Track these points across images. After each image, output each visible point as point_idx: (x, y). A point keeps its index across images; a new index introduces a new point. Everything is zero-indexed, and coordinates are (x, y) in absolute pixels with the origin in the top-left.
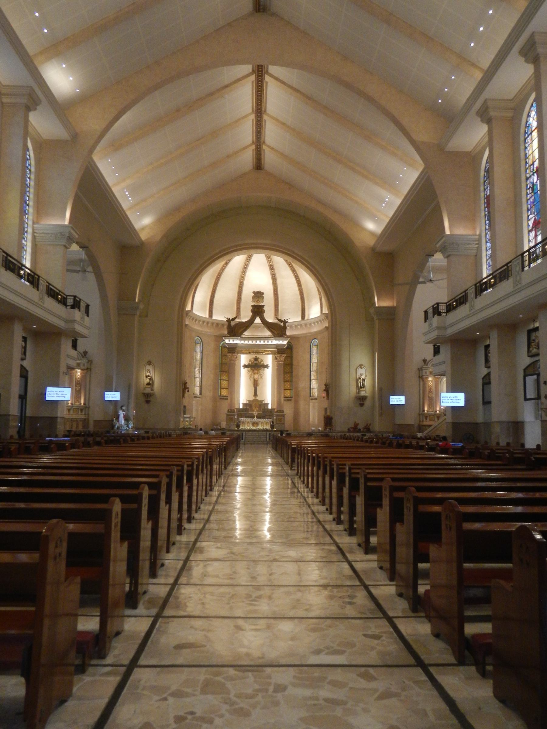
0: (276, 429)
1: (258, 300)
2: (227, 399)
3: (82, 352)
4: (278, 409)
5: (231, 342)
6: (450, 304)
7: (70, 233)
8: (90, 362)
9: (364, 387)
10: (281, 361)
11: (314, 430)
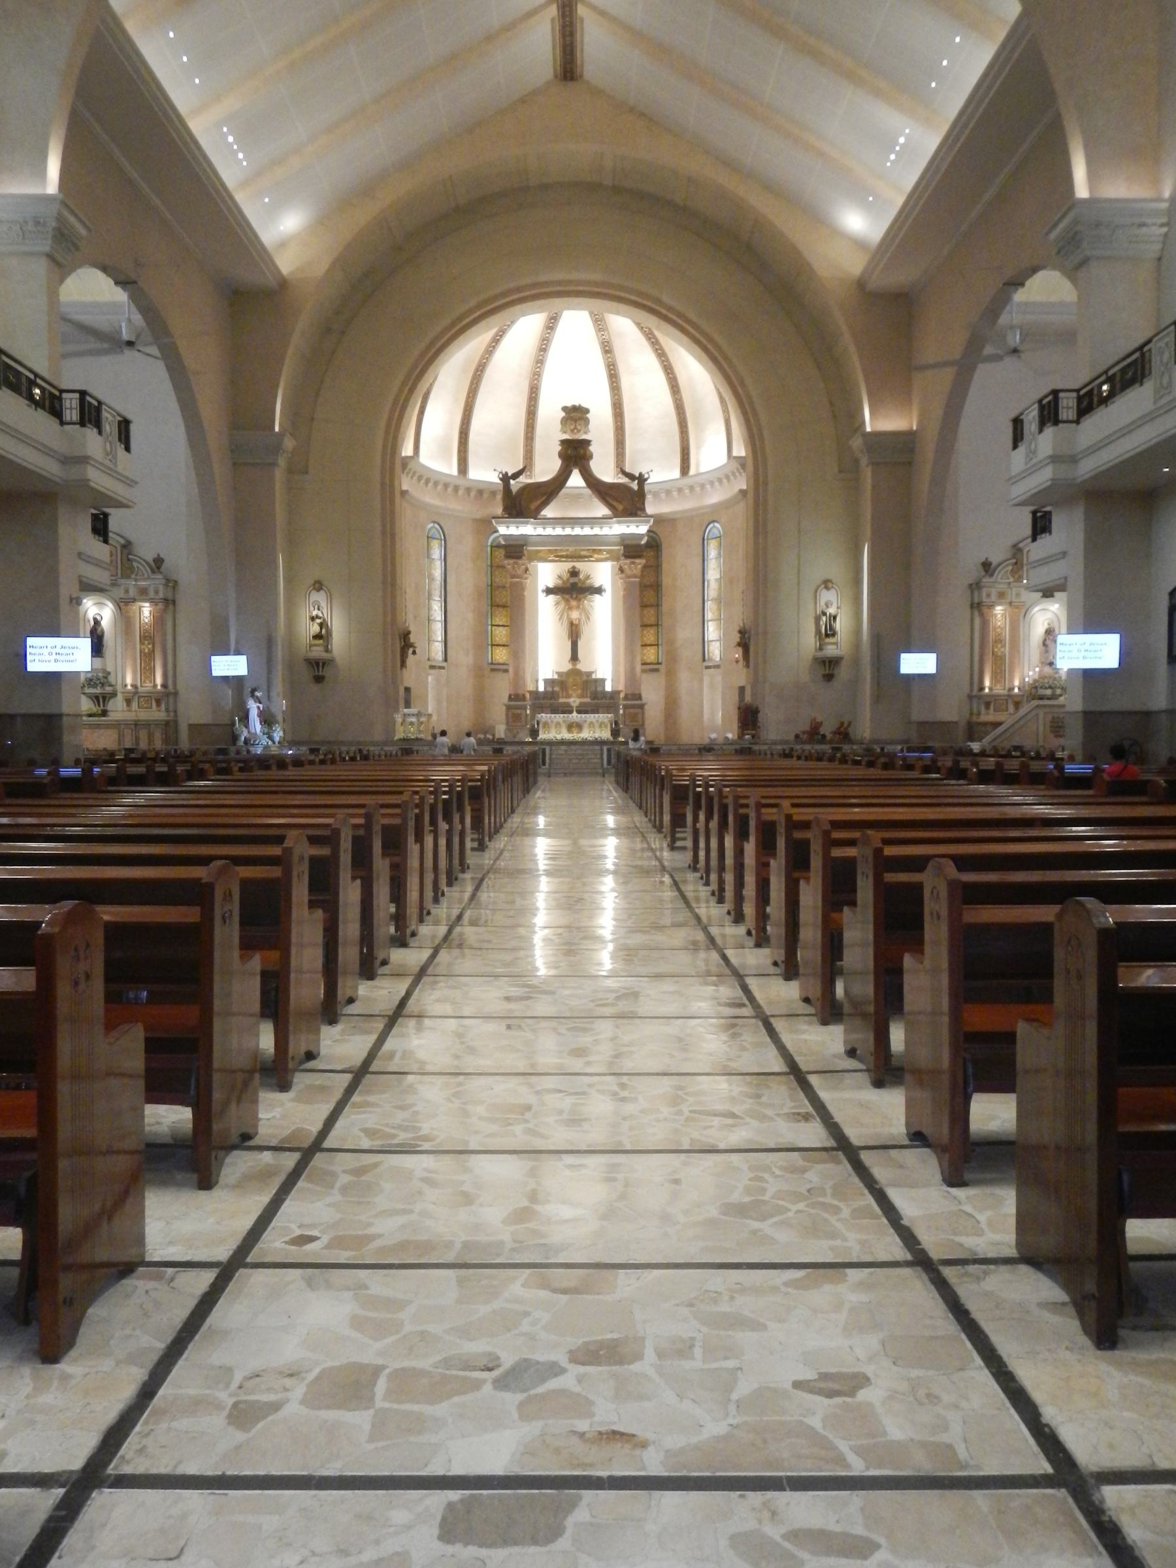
0: (623, 737)
1: (575, 428)
2: (506, 671)
3: (150, 558)
4: (630, 692)
6: (1090, 393)
7: (60, 218)
8: (172, 584)
9: (834, 634)
10: (635, 576)
11: (715, 739)
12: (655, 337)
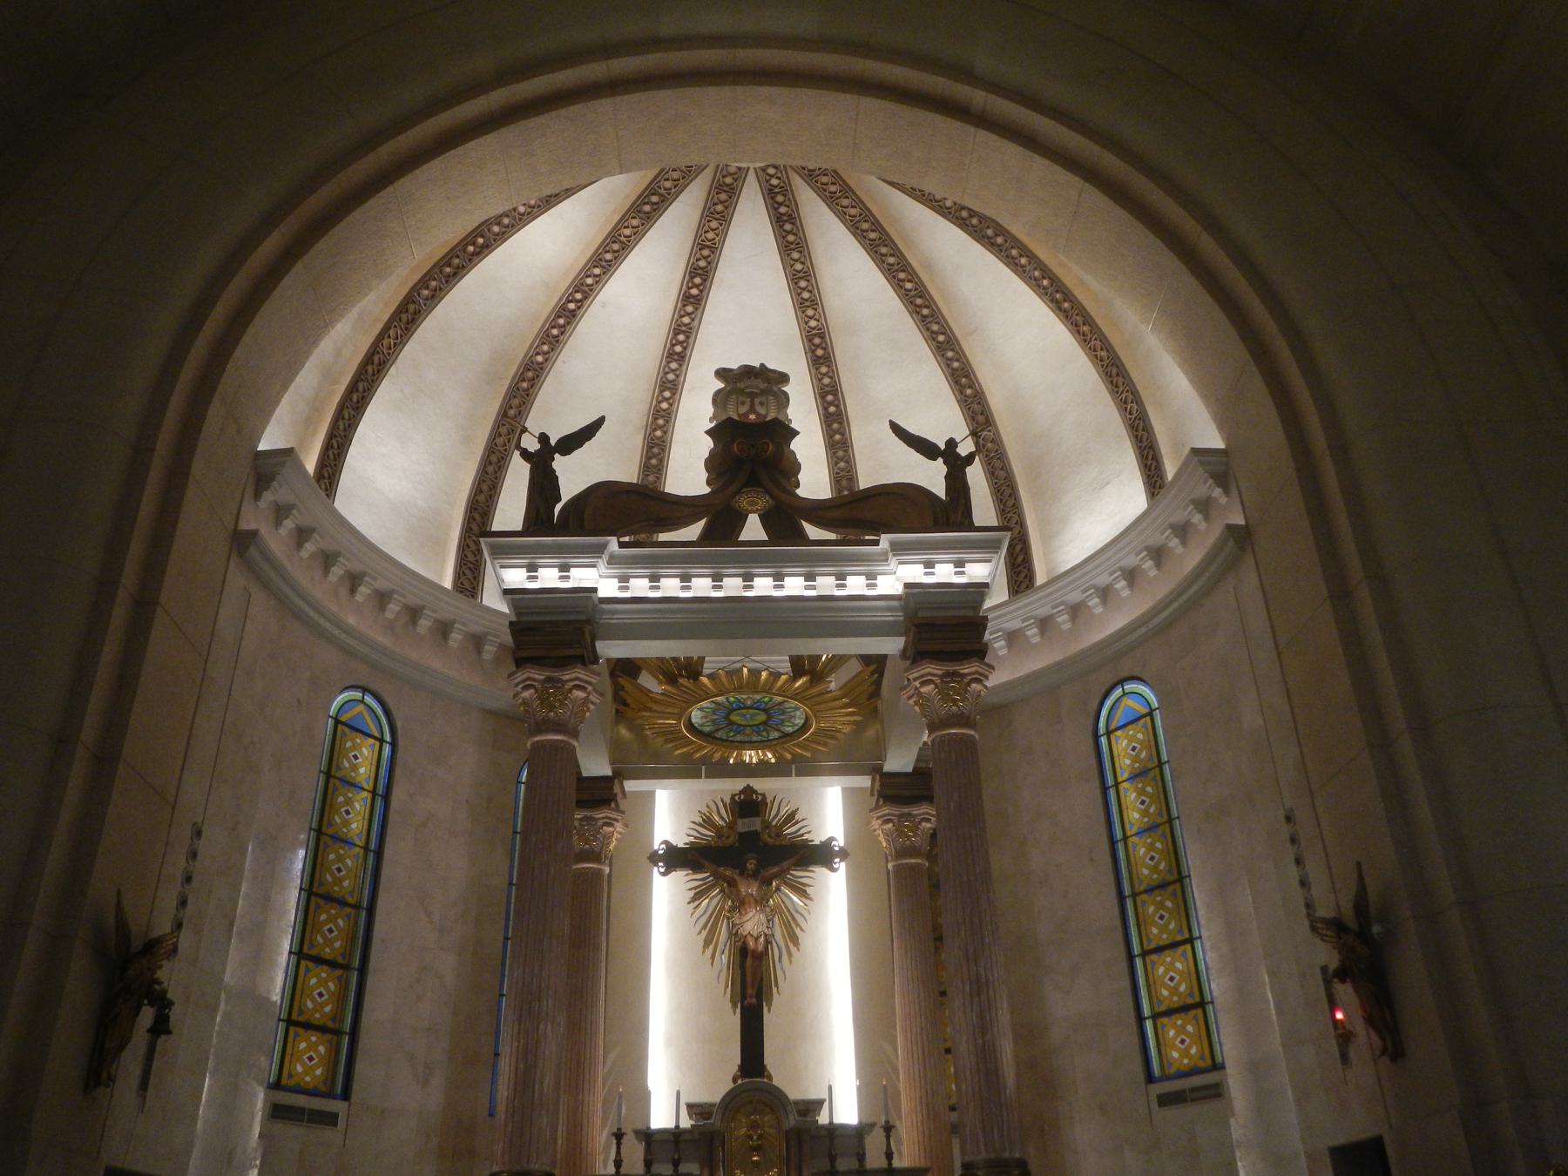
1: (752, 410)
5: (549, 577)
12: (930, 303)
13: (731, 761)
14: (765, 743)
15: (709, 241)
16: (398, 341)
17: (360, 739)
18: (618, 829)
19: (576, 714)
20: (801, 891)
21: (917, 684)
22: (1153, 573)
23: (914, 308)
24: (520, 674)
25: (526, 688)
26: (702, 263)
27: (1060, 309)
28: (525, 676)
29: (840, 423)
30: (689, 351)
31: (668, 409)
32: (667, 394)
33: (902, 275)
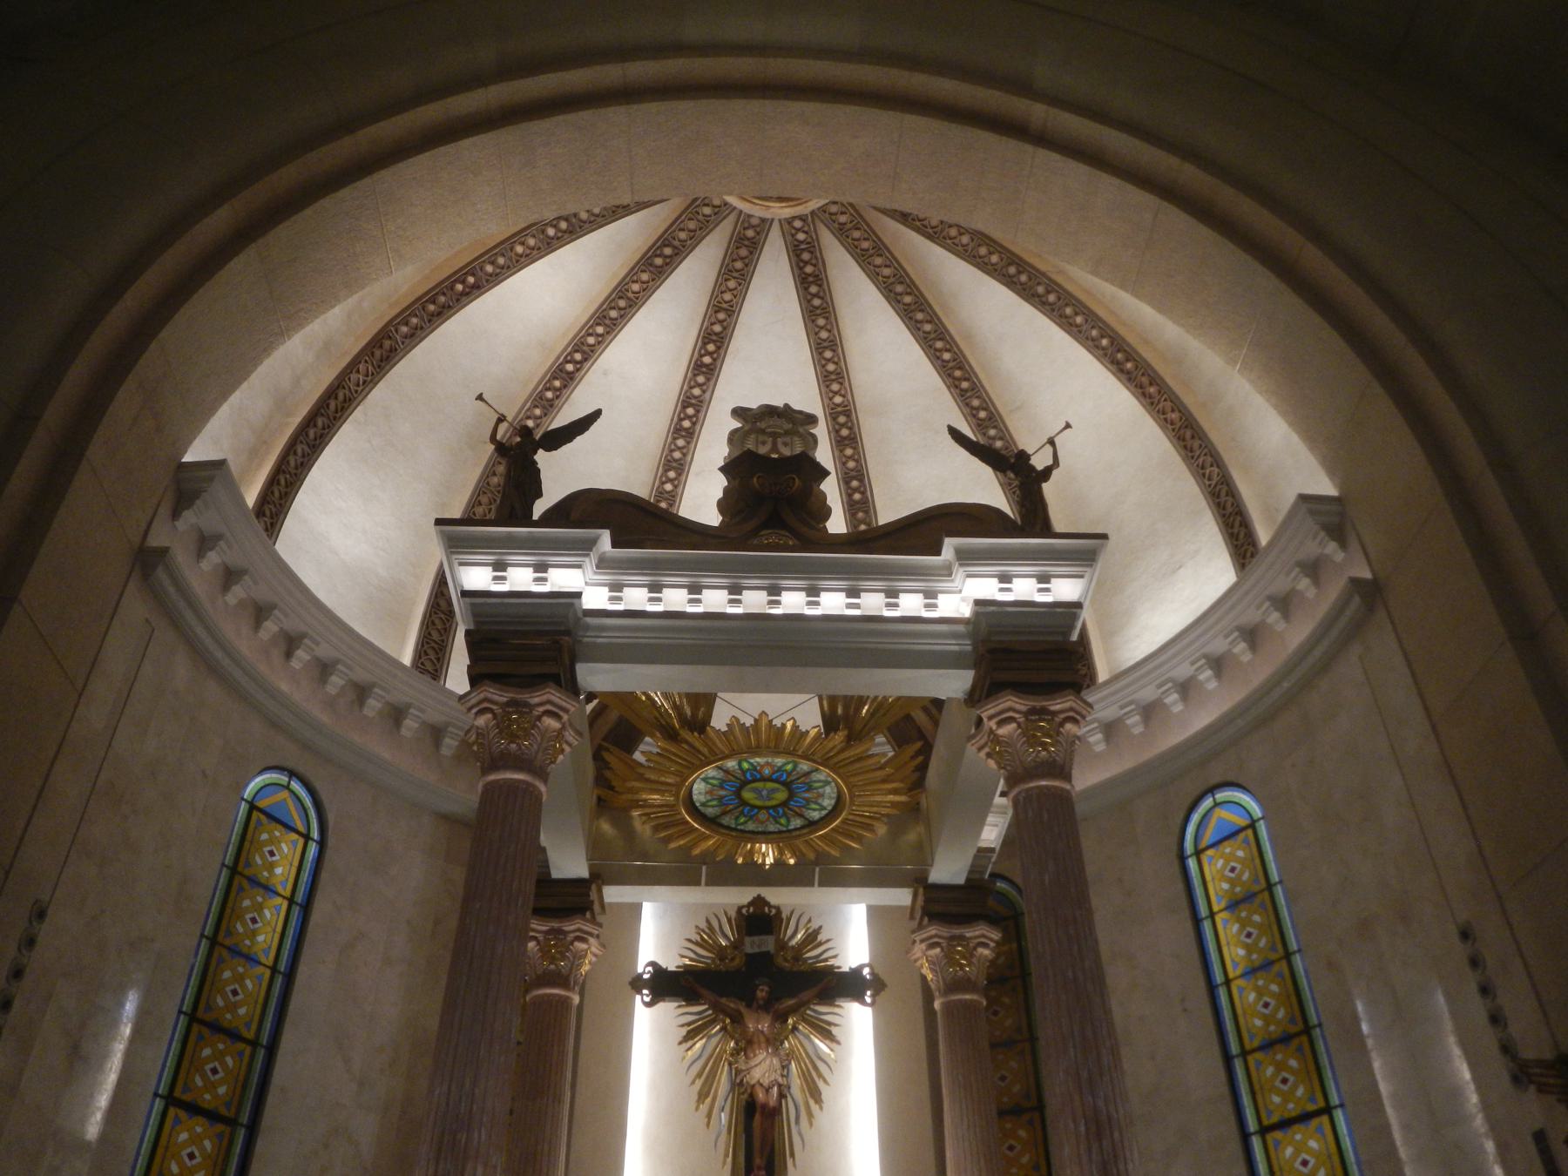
1: (775, 449)
5: (520, 578)
12: (969, 375)
13: (740, 861)
14: (784, 835)
15: (726, 302)
16: (370, 378)
17: (280, 832)
18: (593, 949)
19: (546, 749)
20: (827, 1034)
21: (993, 724)
22: (1247, 657)
23: (951, 380)
24: (475, 693)
25: (481, 712)
26: (717, 328)
27: (1122, 371)
28: (482, 696)
29: (867, 512)
30: (698, 427)
31: (673, 491)
32: (672, 474)
33: (939, 345)
